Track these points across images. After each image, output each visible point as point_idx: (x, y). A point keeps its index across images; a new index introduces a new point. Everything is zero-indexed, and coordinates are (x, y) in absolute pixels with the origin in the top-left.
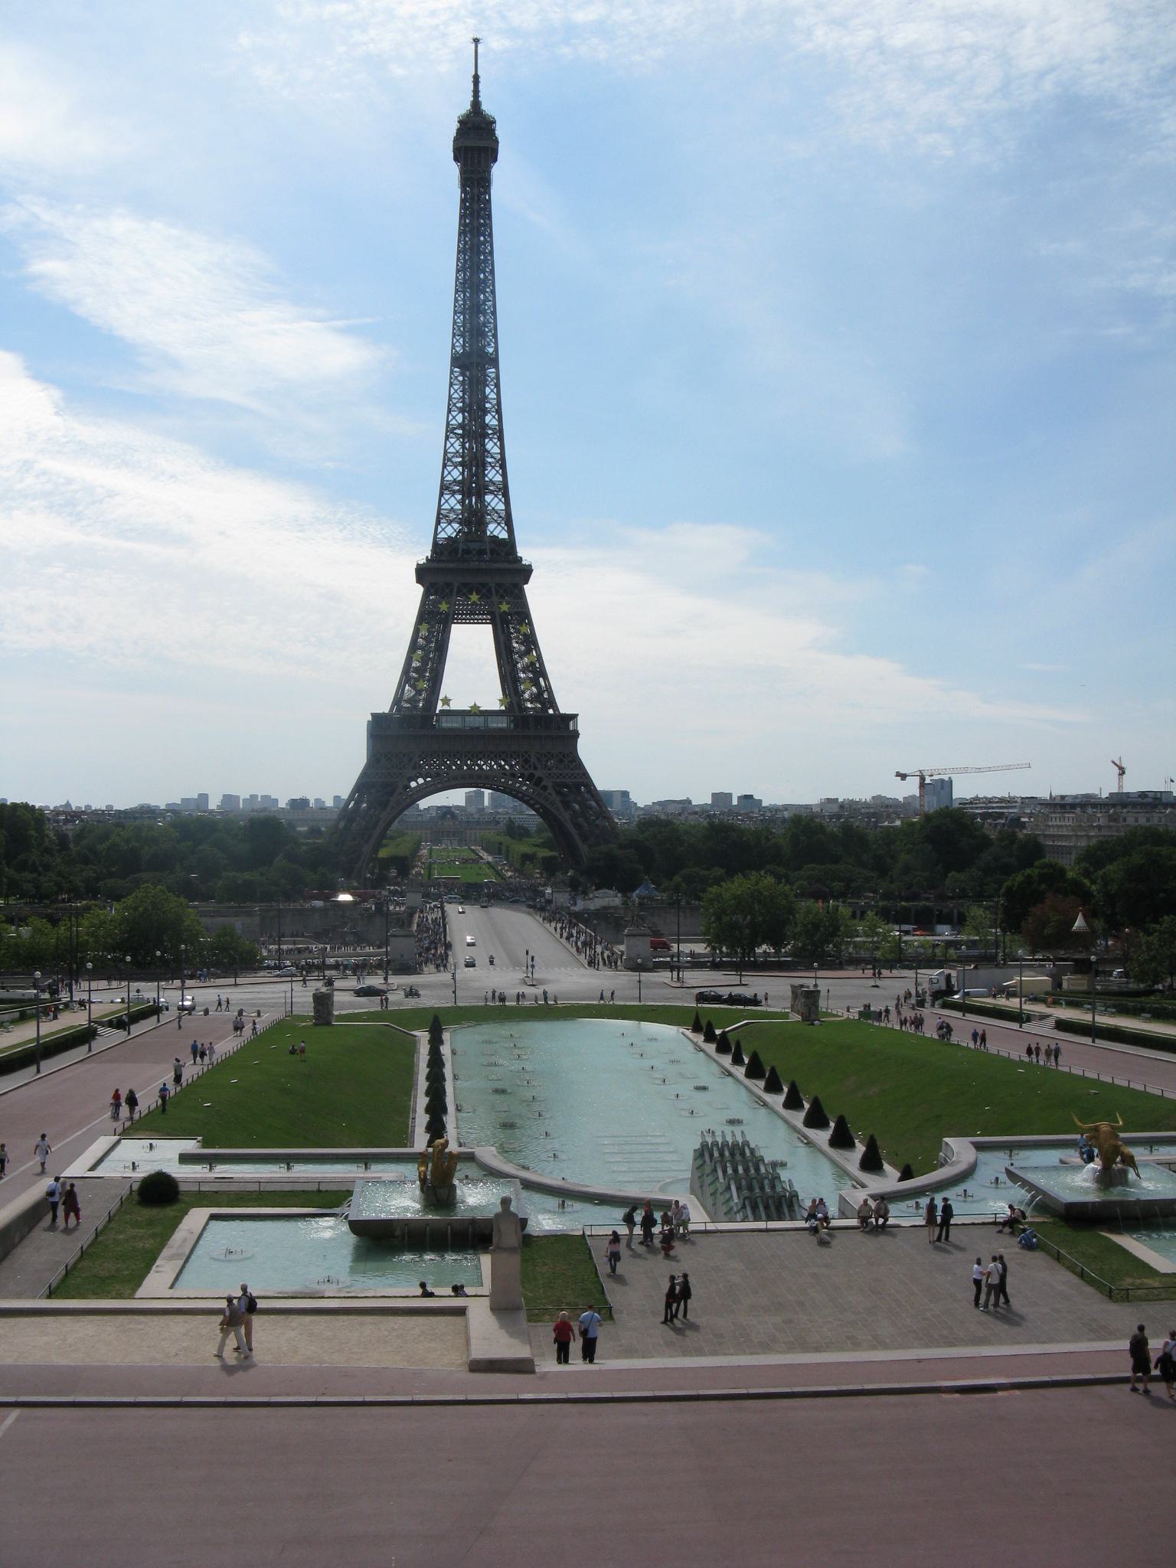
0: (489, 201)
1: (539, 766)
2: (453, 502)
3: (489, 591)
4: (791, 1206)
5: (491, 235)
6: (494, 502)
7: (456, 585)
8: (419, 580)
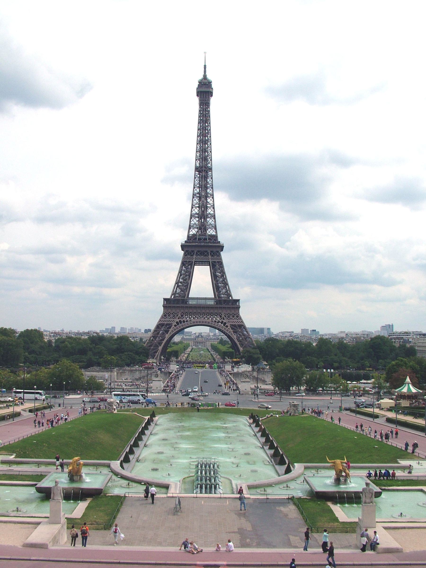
0: (209, 111)
1: (225, 318)
2: (195, 221)
4: (215, 488)
5: (210, 123)
6: (210, 221)
7: (195, 252)
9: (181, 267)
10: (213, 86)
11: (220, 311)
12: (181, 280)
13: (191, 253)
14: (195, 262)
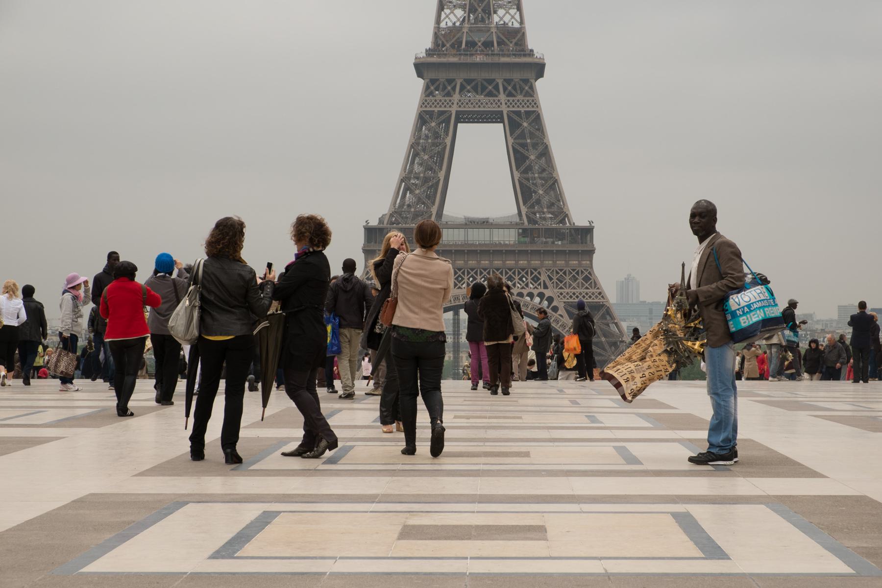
1: (548, 283)
3: (496, 87)
8: (420, 75)
9: (418, 128)
11: (535, 263)
12: (417, 168)
13: (445, 88)
14: (458, 113)
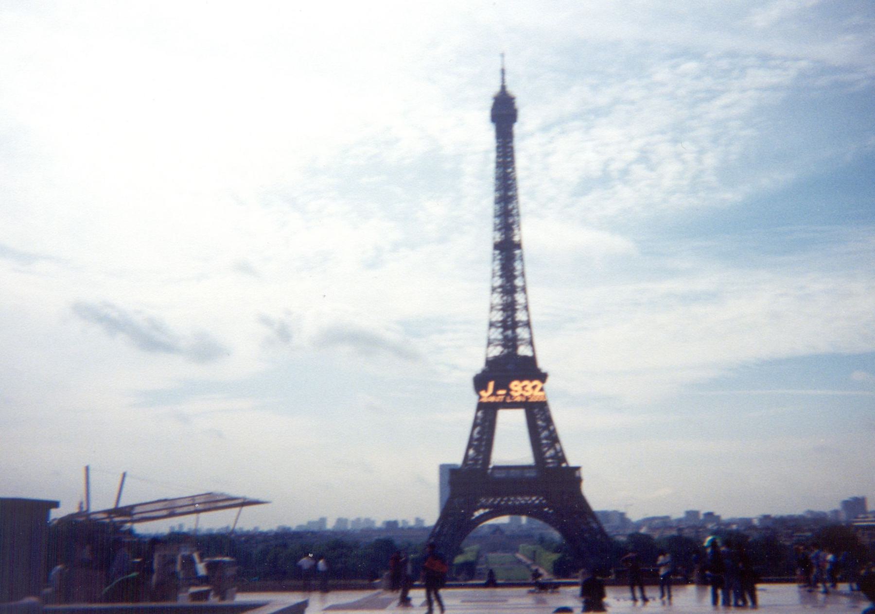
0: (512, 148)
2: (497, 334)
6: (522, 333)
10: (519, 103)
